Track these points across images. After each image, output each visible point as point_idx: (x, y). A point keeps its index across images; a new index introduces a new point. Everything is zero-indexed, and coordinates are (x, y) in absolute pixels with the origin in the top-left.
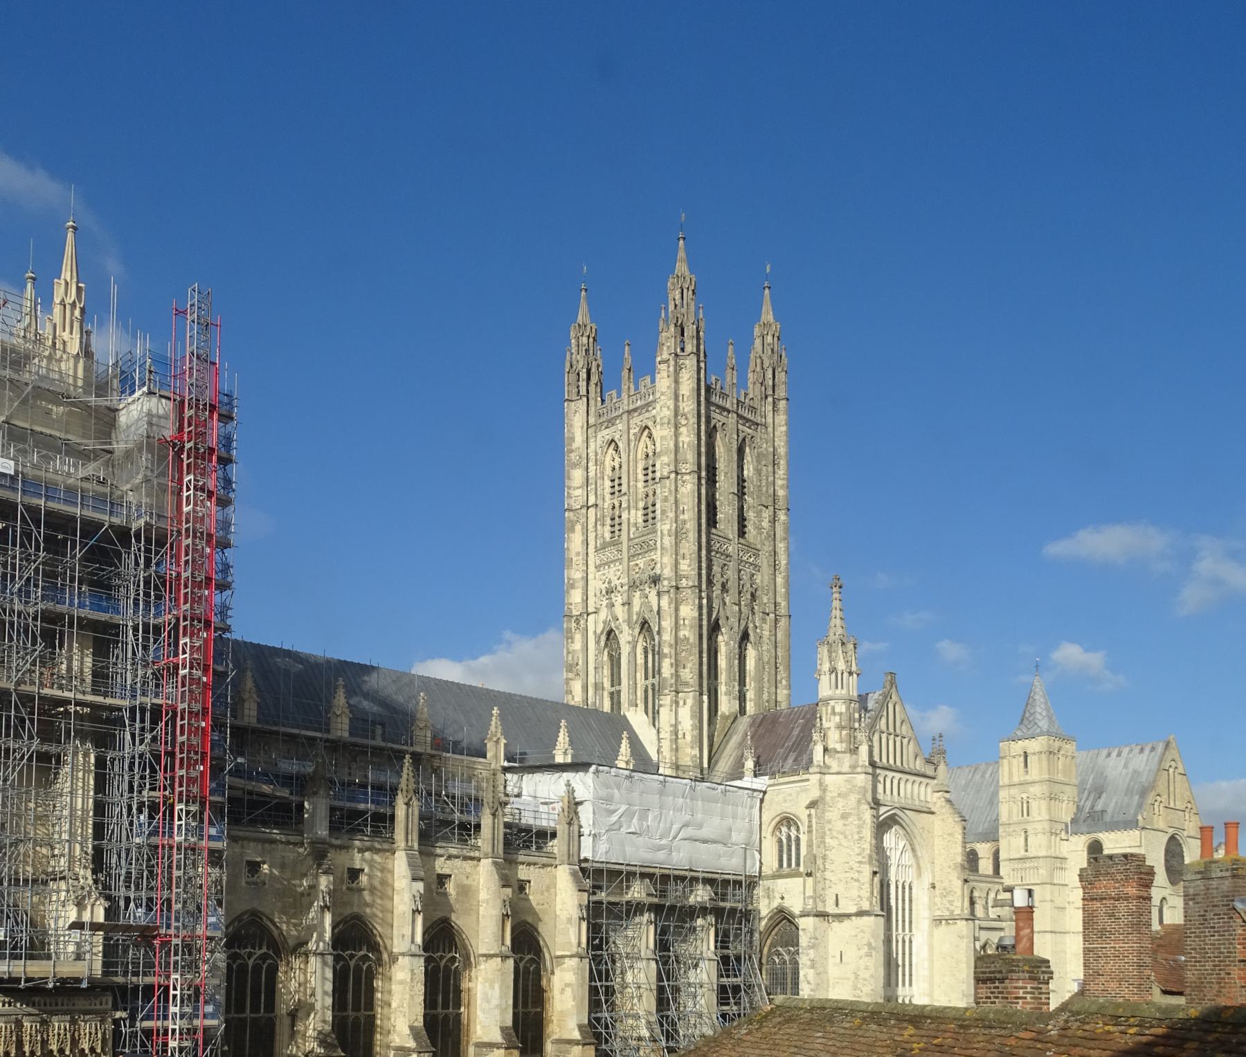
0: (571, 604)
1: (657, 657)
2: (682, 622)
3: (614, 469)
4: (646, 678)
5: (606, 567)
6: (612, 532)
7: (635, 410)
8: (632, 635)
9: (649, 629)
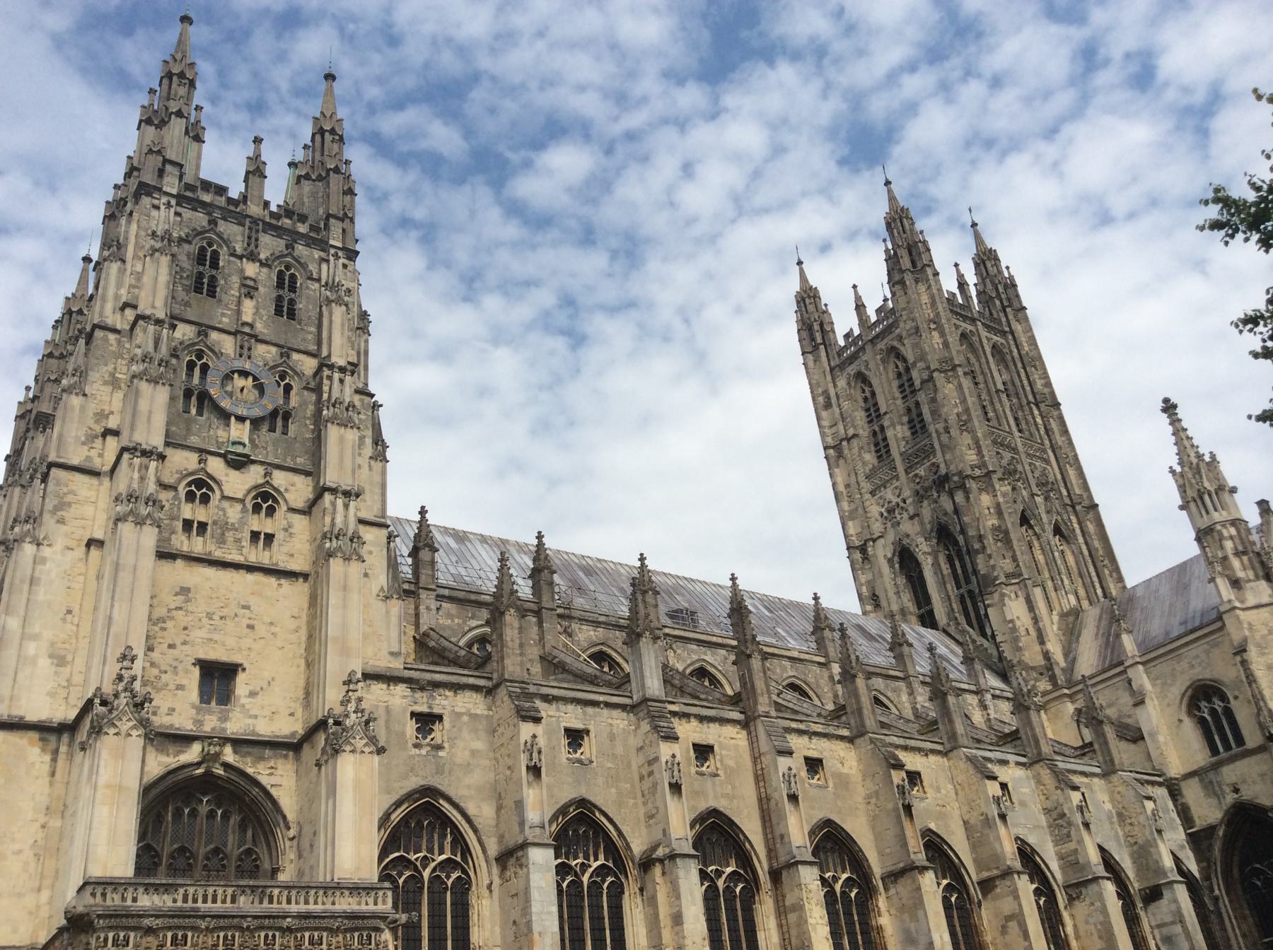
1: (967, 558)
2: (987, 511)
3: (866, 399)
4: (959, 587)
6: (879, 457)
7: (877, 336)
8: (931, 546)
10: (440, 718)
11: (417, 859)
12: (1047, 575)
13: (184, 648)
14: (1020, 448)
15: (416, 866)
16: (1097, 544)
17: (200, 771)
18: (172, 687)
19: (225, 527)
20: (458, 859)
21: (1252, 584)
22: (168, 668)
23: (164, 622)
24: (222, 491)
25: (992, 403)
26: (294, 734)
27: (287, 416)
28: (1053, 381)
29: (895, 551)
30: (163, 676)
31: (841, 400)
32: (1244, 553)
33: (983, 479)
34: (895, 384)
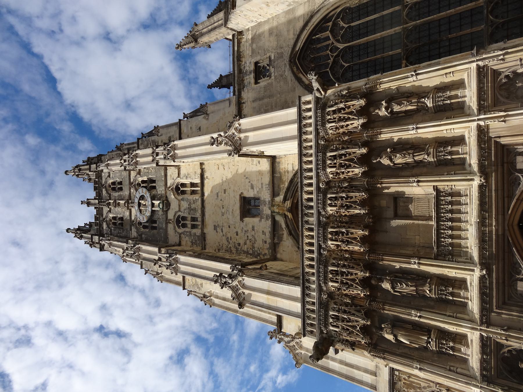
10: (256, 63)
11: (332, 56)
13: (237, 227)
15: (336, 56)
17: (290, 215)
18: (253, 233)
19: (190, 209)
20: (330, 24)
22: (246, 235)
23: (228, 238)
24: (178, 212)
26: (268, 161)
27: (154, 181)
30: (249, 238)
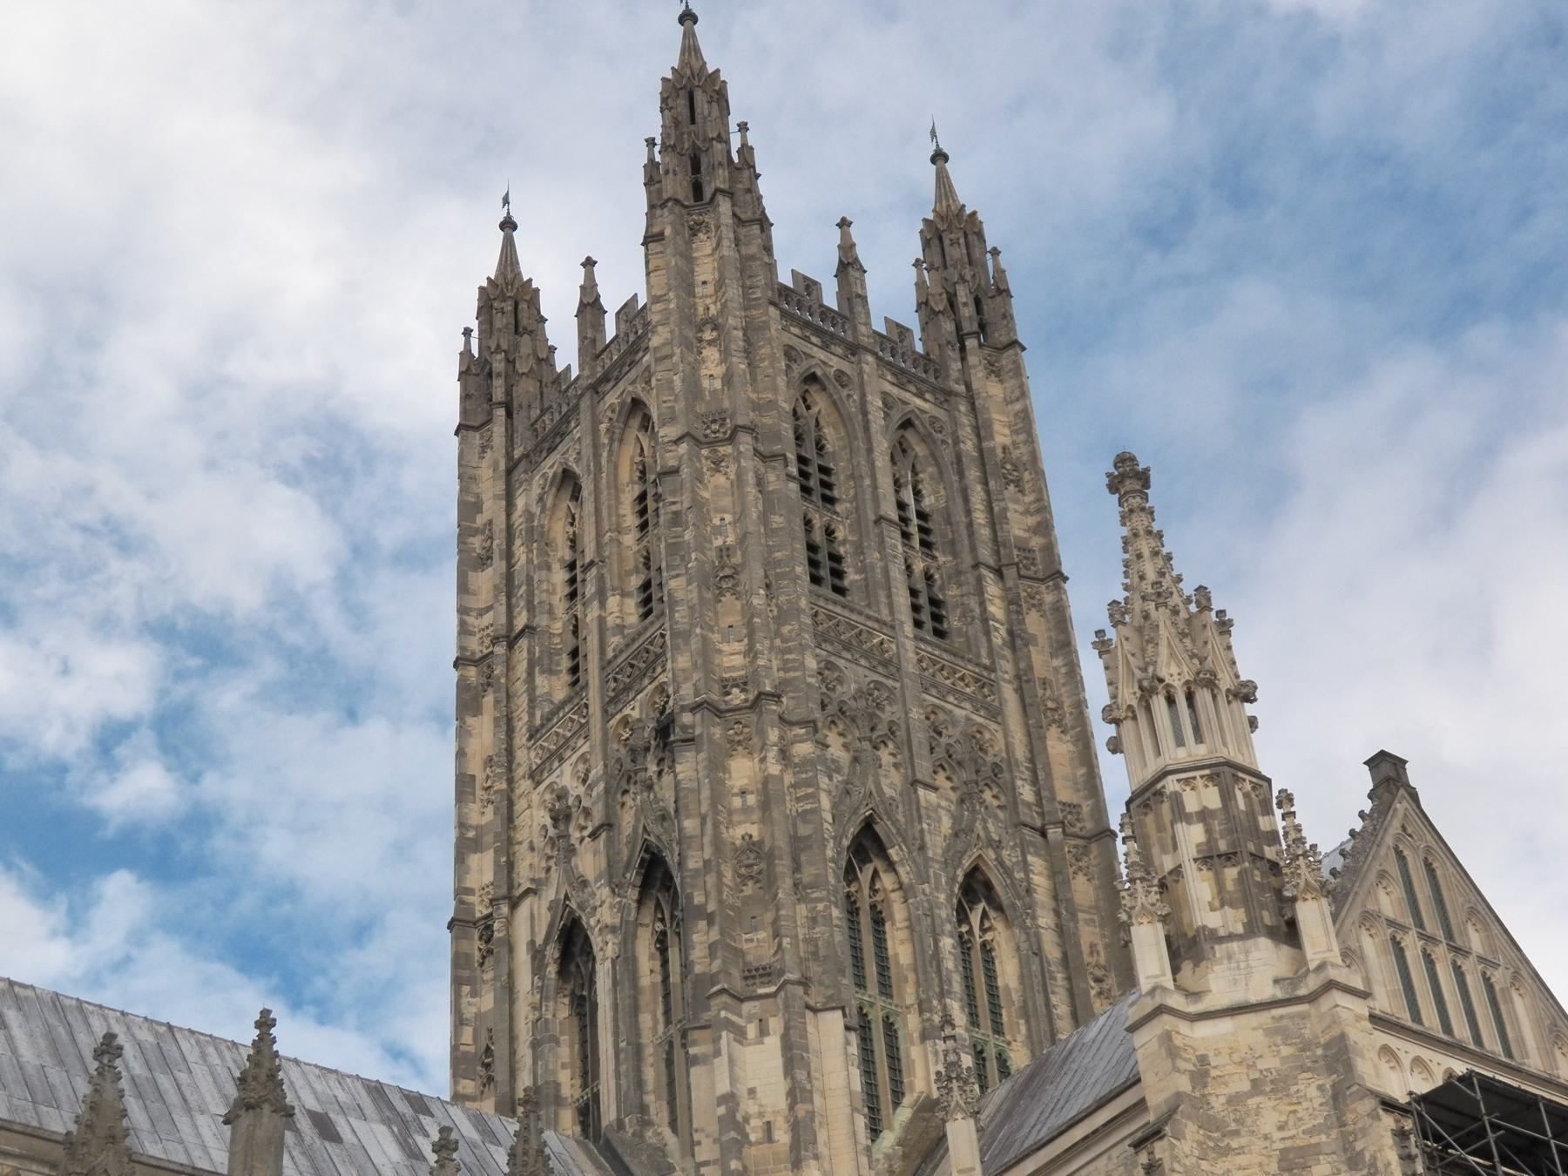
0: (470, 891)
4: (668, 1022)
5: (556, 764)
7: (605, 379)
9: (668, 883)
12: (910, 998)
14: (910, 667)
16: (1089, 934)
21: (1235, 946)
25: (859, 550)
28: (1057, 522)
29: (551, 926)
31: (518, 542)
32: (1230, 857)
33: (744, 717)
34: (630, 494)
